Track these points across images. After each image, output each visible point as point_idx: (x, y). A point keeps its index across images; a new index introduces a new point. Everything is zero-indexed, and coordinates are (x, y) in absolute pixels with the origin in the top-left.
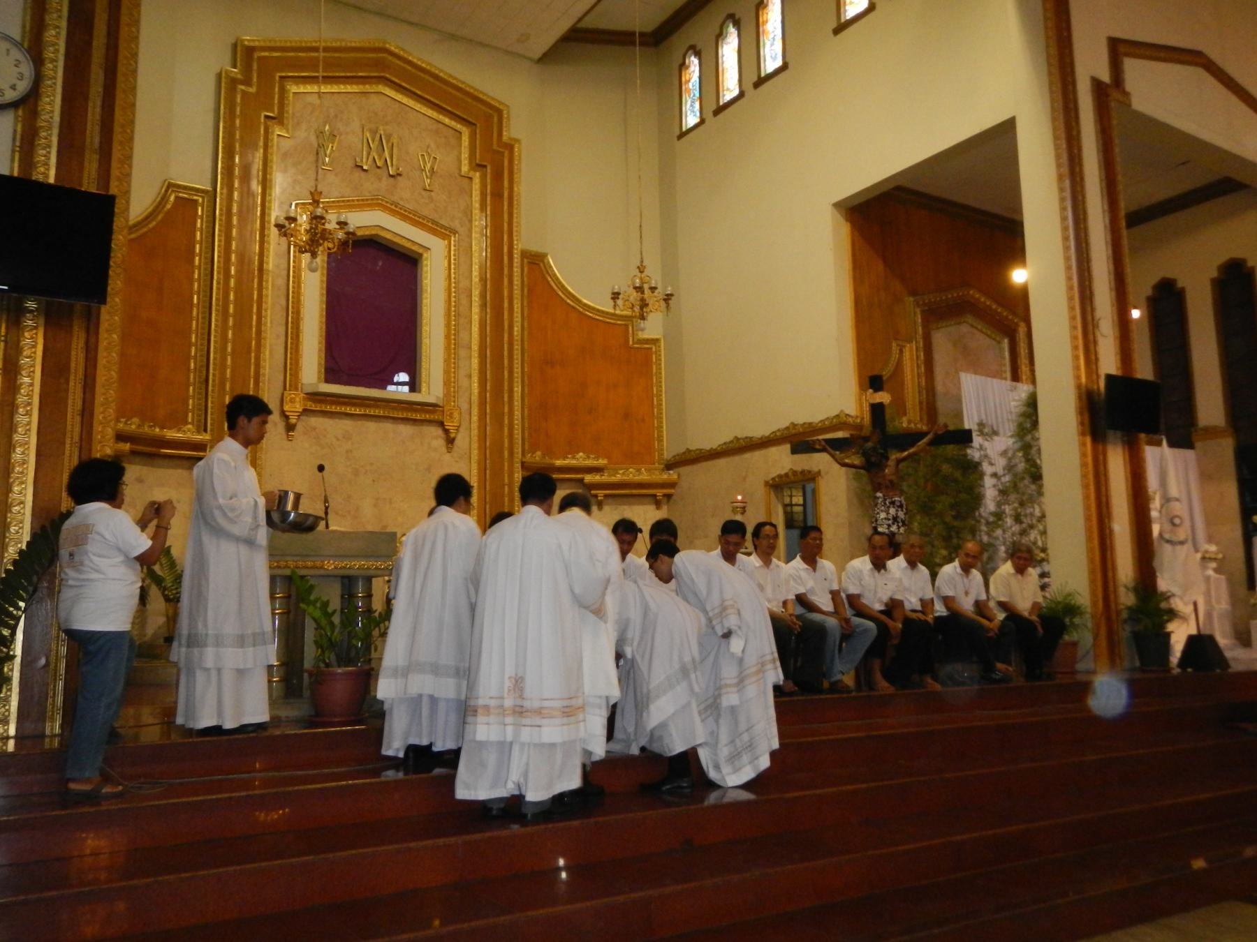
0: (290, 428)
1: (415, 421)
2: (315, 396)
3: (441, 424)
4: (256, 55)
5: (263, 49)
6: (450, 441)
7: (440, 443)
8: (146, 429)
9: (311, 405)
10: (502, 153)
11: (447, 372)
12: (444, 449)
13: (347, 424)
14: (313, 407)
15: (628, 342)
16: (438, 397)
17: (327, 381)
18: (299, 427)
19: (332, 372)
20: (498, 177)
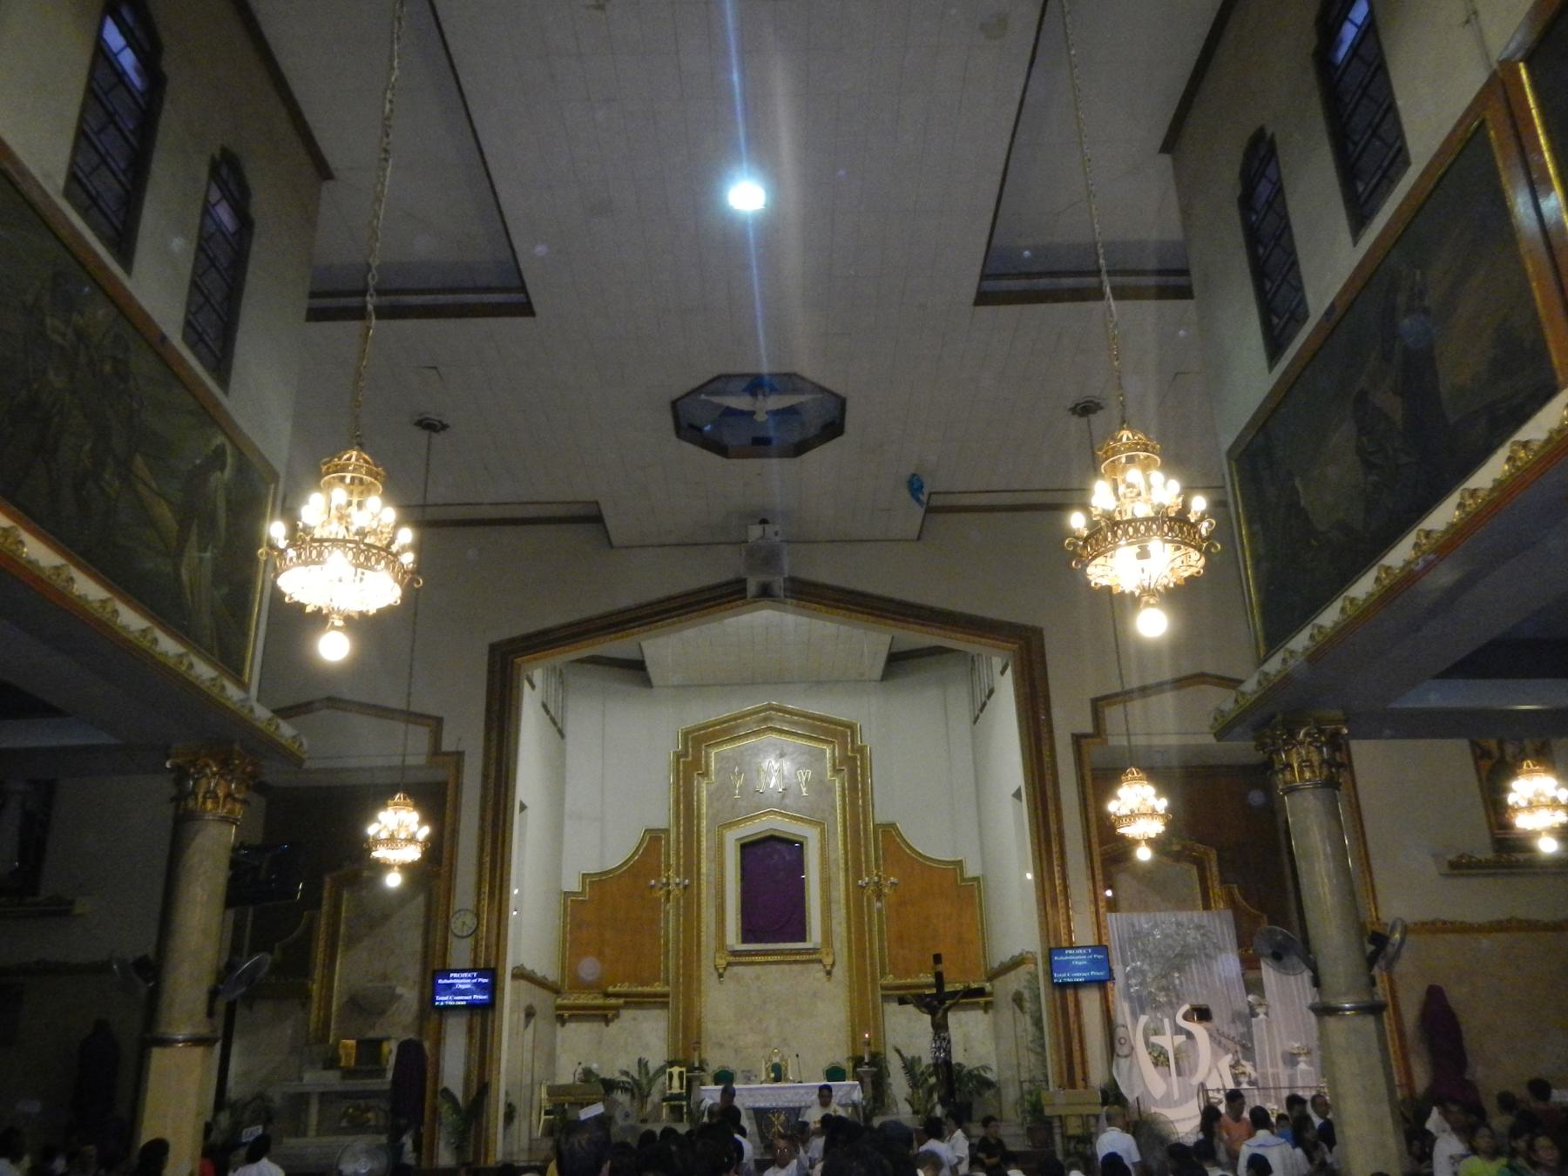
0: (721, 976)
1: (803, 962)
2: (735, 953)
3: (820, 961)
4: (690, 737)
5: (694, 731)
6: (829, 973)
7: (822, 975)
8: (634, 989)
9: (732, 959)
10: (854, 759)
11: (823, 921)
12: (825, 979)
13: (758, 968)
14: (732, 959)
15: (956, 880)
16: (816, 944)
17: (745, 940)
18: (727, 974)
19: (748, 934)
20: (853, 774)
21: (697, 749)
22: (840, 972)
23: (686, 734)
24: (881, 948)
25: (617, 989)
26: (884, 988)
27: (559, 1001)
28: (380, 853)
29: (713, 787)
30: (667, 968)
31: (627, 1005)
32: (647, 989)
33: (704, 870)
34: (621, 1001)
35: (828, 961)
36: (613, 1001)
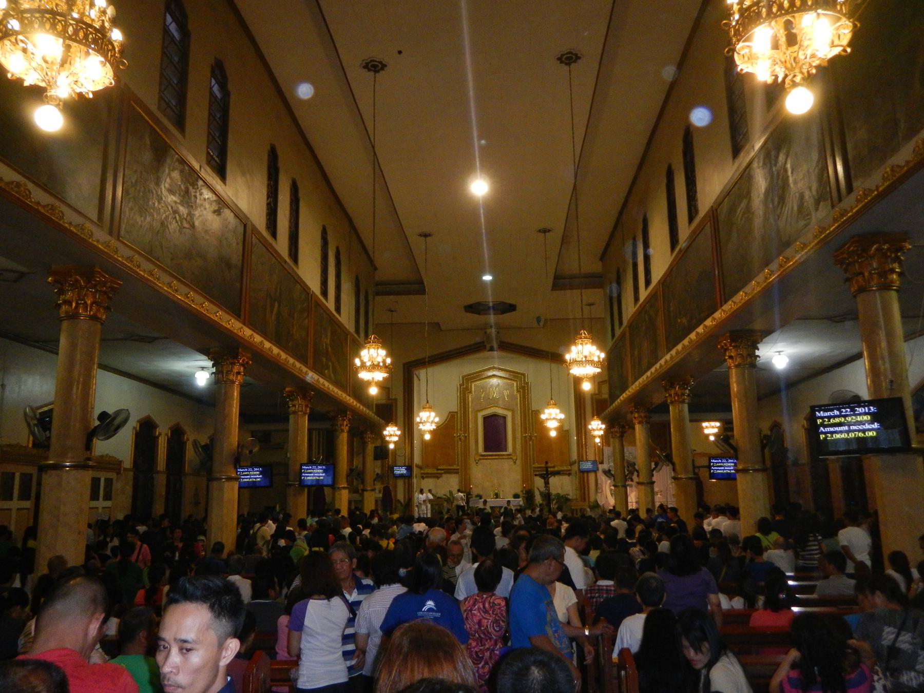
0: (477, 463)
2: (482, 456)
3: (512, 458)
6: (515, 462)
7: (512, 463)
17: (485, 451)
21: (467, 383)
22: (518, 462)
23: (463, 377)
24: (533, 454)
25: (441, 467)
26: (535, 468)
27: (422, 471)
28: (388, 438)
29: (473, 396)
30: (458, 460)
31: (445, 473)
32: (452, 467)
33: (470, 426)
34: (443, 471)
35: (515, 458)
36: (440, 472)
